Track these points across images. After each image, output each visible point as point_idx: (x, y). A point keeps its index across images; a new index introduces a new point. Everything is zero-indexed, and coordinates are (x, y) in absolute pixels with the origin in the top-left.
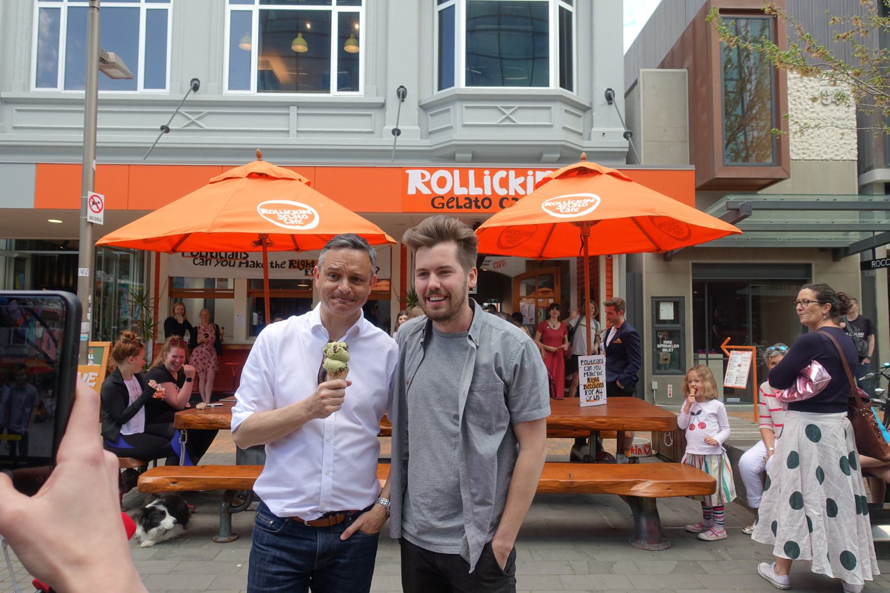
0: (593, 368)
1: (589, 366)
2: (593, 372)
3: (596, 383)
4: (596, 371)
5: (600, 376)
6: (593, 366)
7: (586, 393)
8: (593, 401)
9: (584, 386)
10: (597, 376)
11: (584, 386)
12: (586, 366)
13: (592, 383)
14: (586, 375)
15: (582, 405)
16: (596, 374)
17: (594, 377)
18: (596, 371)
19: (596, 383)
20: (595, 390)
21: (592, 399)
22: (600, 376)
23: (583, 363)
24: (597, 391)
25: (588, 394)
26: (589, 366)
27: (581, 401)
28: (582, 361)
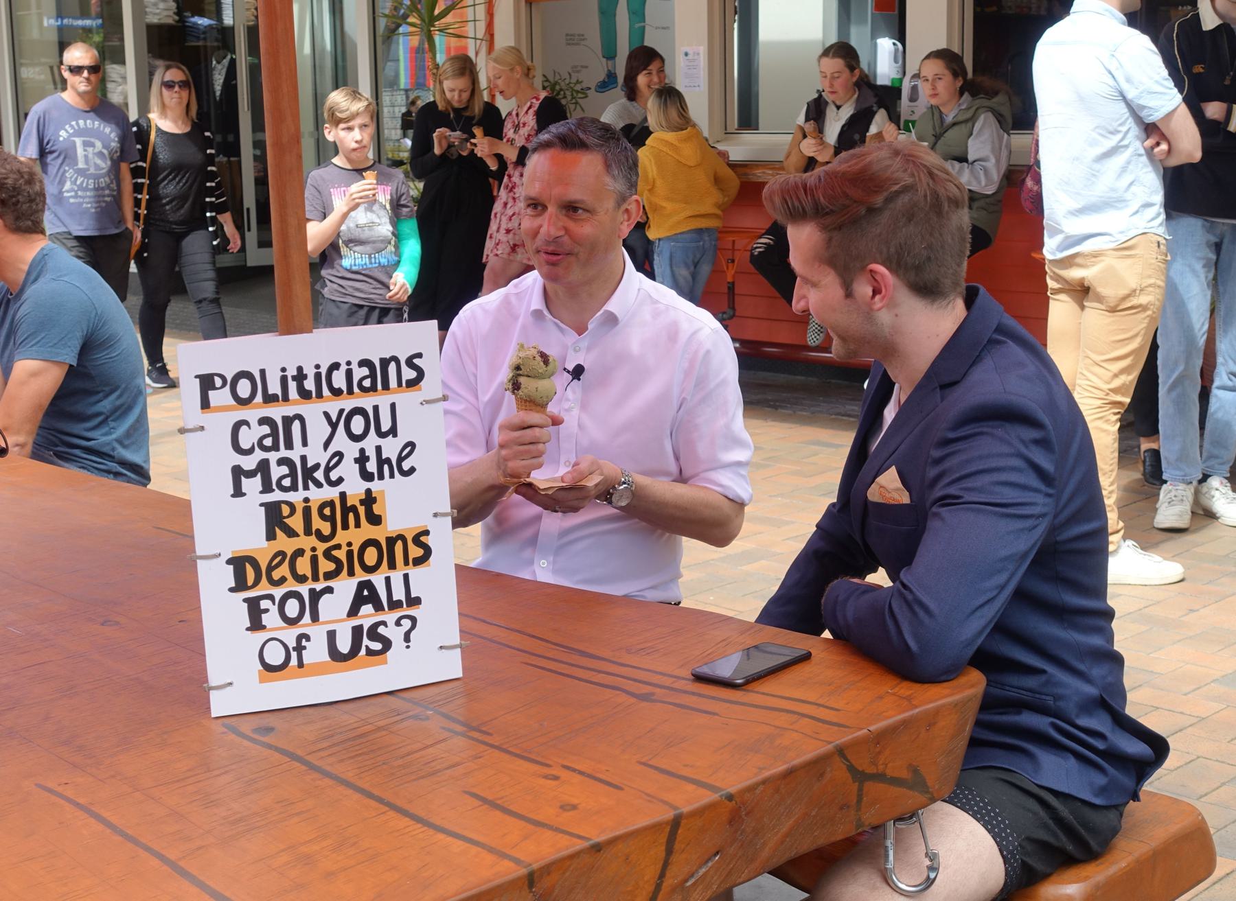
0: (318, 430)
1: (277, 412)
2: (317, 455)
3: (354, 536)
4: (351, 450)
5: (389, 490)
6: (313, 412)
7: (253, 605)
8: (319, 669)
9: (239, 563)
10: (355, 487)
11: (239, 563)
12: (252, 414)
13: (307, 542)
14: (252, 485)
15: (221, 704)
16: (348, 469)
17: (331, 493)
18: (351, 450)
19: (354, 536)
20: (345, 588)
21: (316, 652)
22: (389, 490)
23: (220, 397)
24: (365, 596)
25: (271, 618)
26: (277, 412)
27: (214, 678)
28: (207, 382)
